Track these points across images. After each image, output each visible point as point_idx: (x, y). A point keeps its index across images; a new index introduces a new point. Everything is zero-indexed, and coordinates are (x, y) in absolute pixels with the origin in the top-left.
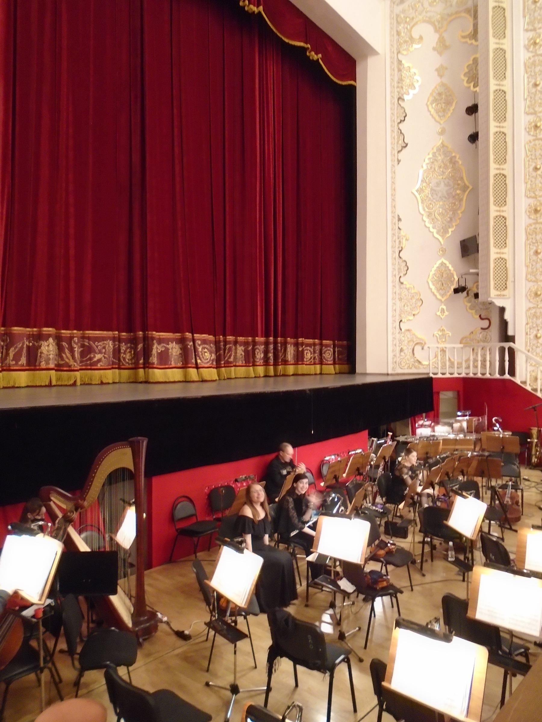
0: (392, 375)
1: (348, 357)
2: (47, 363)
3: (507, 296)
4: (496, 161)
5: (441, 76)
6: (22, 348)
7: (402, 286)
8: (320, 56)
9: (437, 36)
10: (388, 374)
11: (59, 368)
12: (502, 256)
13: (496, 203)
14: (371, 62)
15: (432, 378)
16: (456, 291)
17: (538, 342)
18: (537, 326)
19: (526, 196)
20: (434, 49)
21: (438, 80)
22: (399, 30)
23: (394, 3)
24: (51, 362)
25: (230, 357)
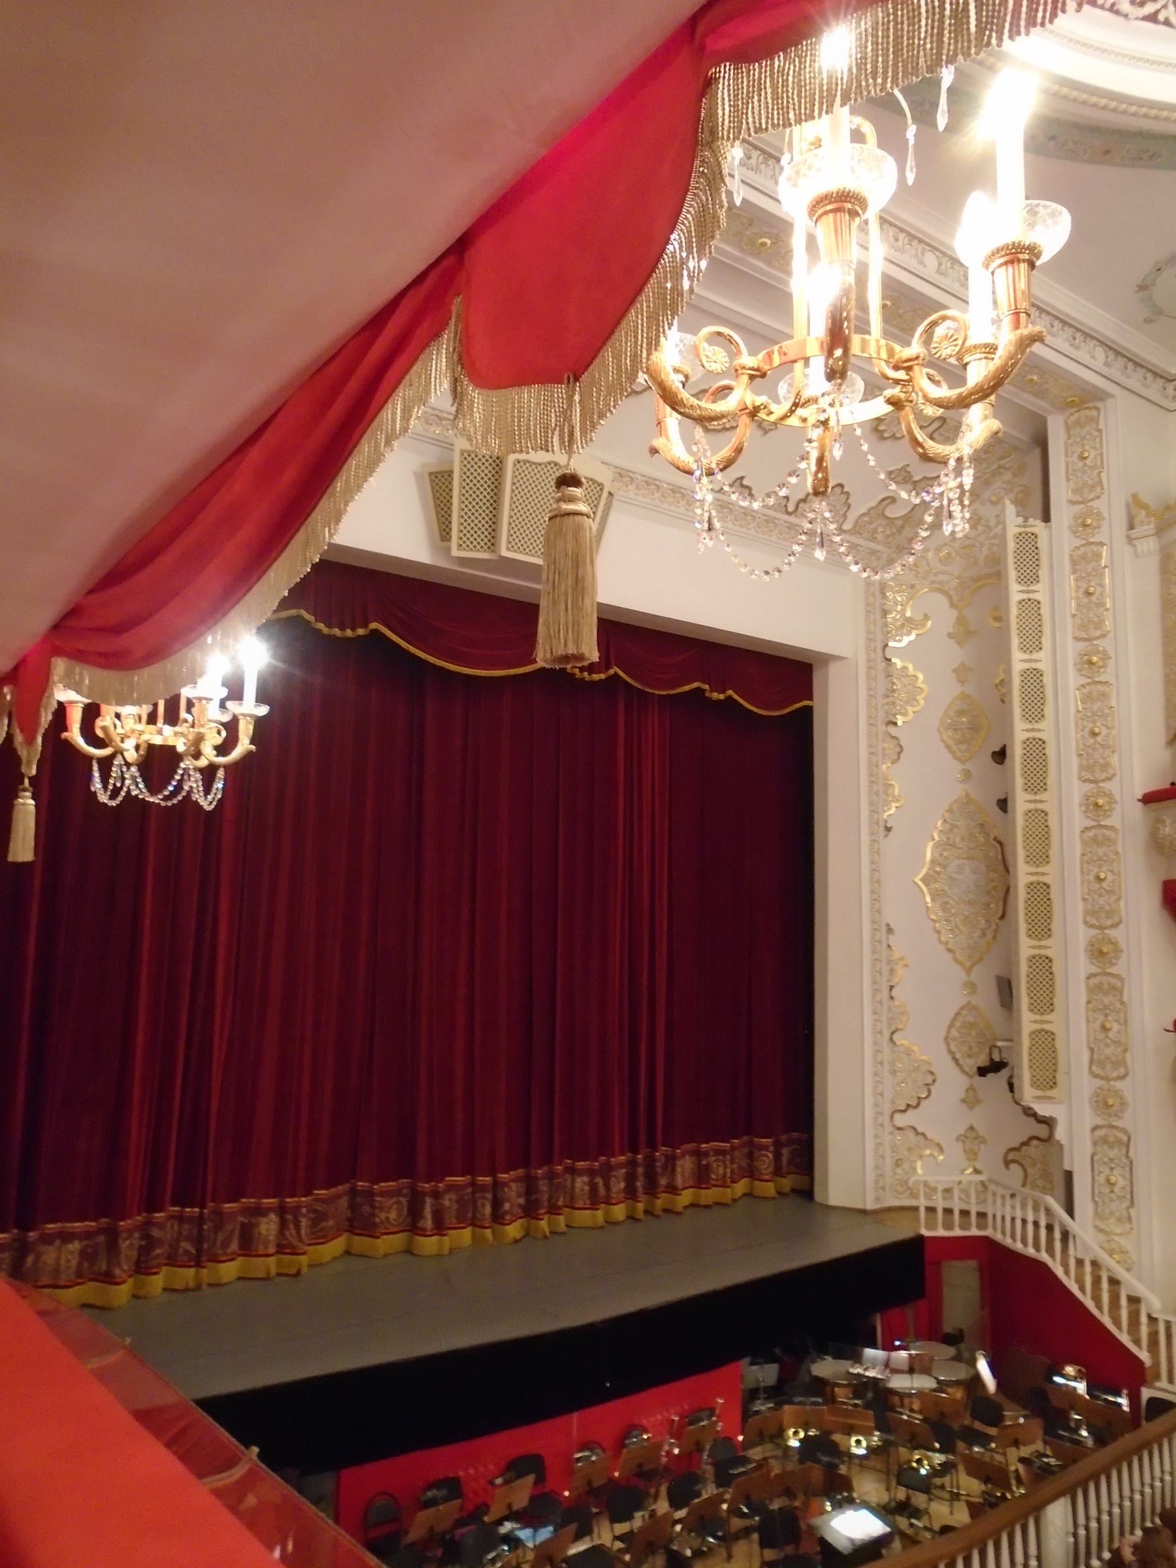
2: (266, 1248)
4: (1029, 860)
6: (233, 1231)
7: (896, 1049)
9: (954, 613)
11: (281, 1249)
12: (1046, 1027)
14: (833, 668)
15: (920, 1239)
16: (982, 1072)
17: (1112, 1192)
18: (1111, 1160)
19: (1086, 923)
20: (950, 635)
21: (957, 689)
22: (885, 607)
24: (270, 1245)
25: (557, 1200)
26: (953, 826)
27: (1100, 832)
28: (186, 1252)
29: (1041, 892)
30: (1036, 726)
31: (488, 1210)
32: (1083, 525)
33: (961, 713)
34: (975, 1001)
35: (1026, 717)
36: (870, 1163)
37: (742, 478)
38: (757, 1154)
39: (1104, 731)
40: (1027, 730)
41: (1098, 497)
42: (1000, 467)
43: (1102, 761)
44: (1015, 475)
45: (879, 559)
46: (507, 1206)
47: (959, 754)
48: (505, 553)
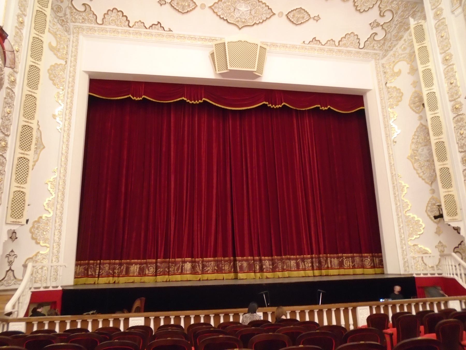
0: (403, 275)
1: (379, 263)
3: (459, 220)
5: (415, 87)
8: (329, 107)
9: (409, 65)
10: (400, 275)
12: (450, 193)
13: (439, 160)
16: (436, 217)
20: (409, 73)
22: (385, 71)
23: (378, 60)
26: (418, 136)
27: (458, 117)
28: (166, 271)
29: (441, 146)
30: (431, 88)
31: (258, 267)
32: (437, 15)
33: (415, 97)
34: (435, 196)
35: (426, 86)
36: (400, 258)
37: (315, 38)
38: (364, 259)
39: (455, 81)
40: (428, 90)
41: (440, 4)
42: (414, 12)
43: (456, 92)
44: (421, 13)
45: (379, 56)
46: (264, 267)
47: (417, 111)
48: (229, 68)
